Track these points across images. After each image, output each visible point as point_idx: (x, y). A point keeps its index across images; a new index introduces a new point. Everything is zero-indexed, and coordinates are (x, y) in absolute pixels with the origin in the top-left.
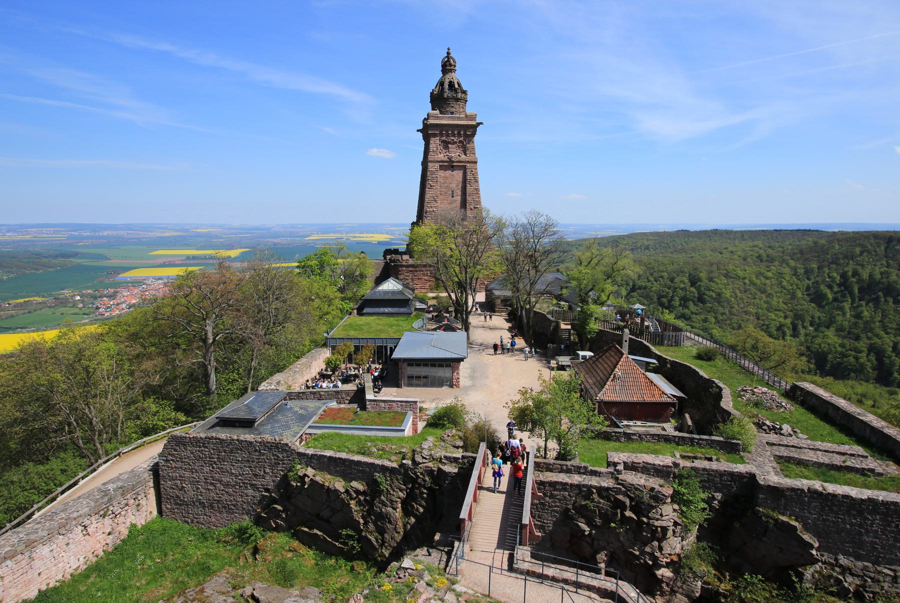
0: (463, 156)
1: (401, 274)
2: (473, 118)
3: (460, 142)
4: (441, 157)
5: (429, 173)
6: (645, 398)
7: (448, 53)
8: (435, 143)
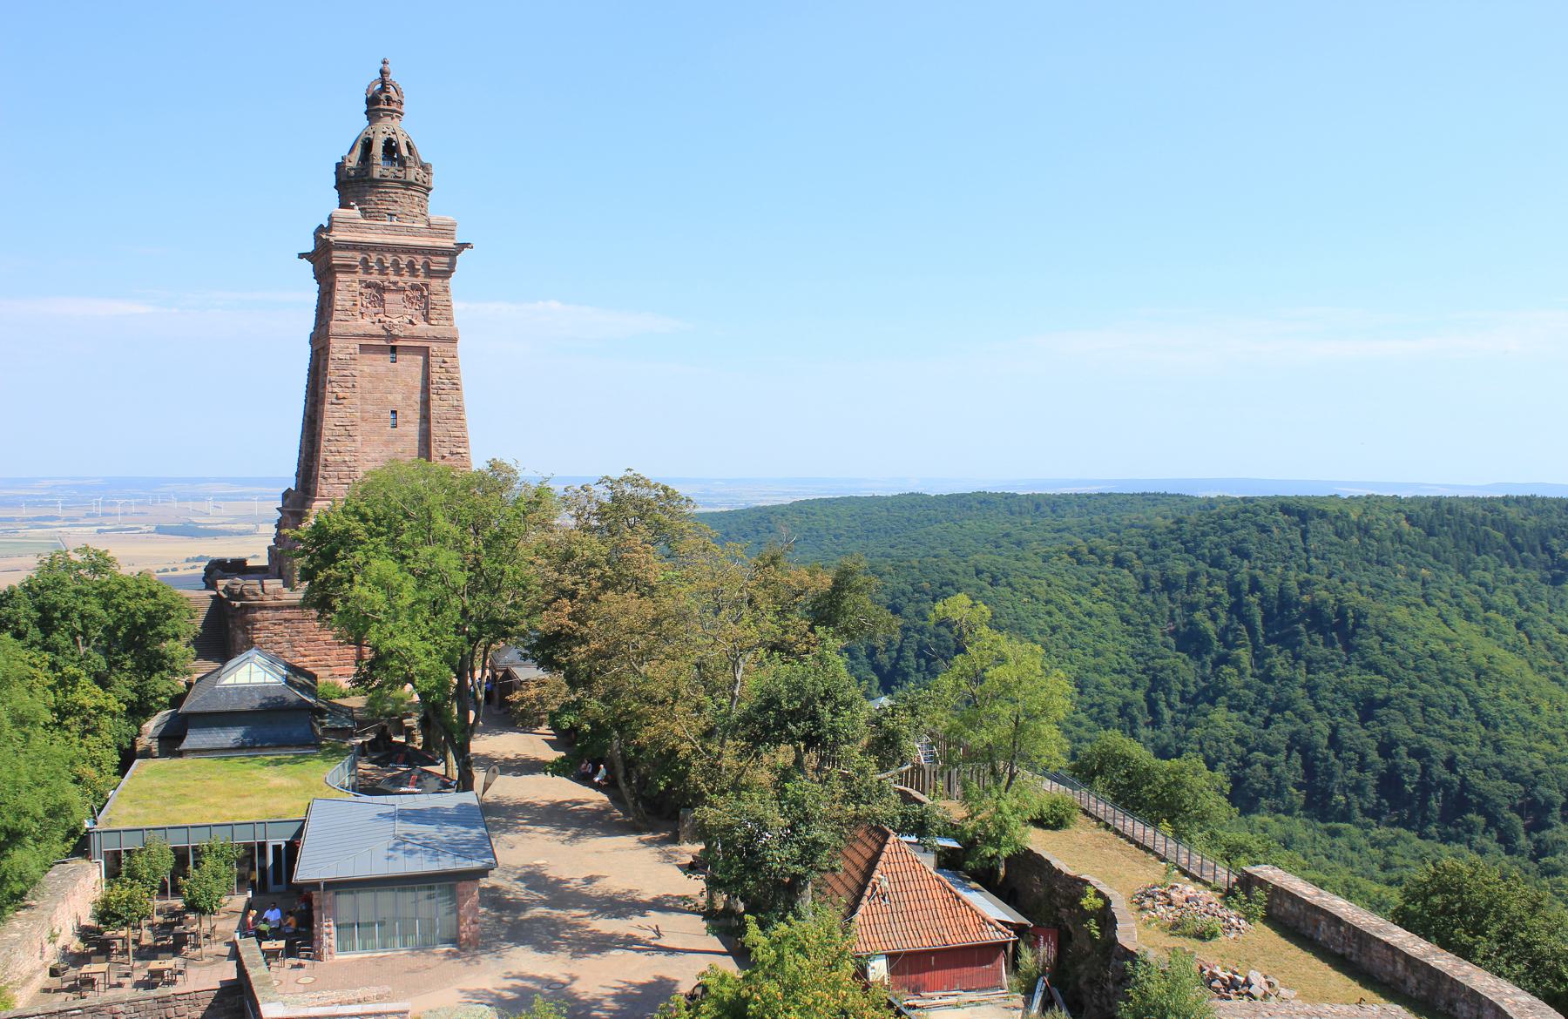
0: (421, 327)
2: (446, 230)
3: (414, 287)
4: (365, 324)
5: (331, 366)
6: (948, 938)
7: (382, 72)
8: (347, 288)
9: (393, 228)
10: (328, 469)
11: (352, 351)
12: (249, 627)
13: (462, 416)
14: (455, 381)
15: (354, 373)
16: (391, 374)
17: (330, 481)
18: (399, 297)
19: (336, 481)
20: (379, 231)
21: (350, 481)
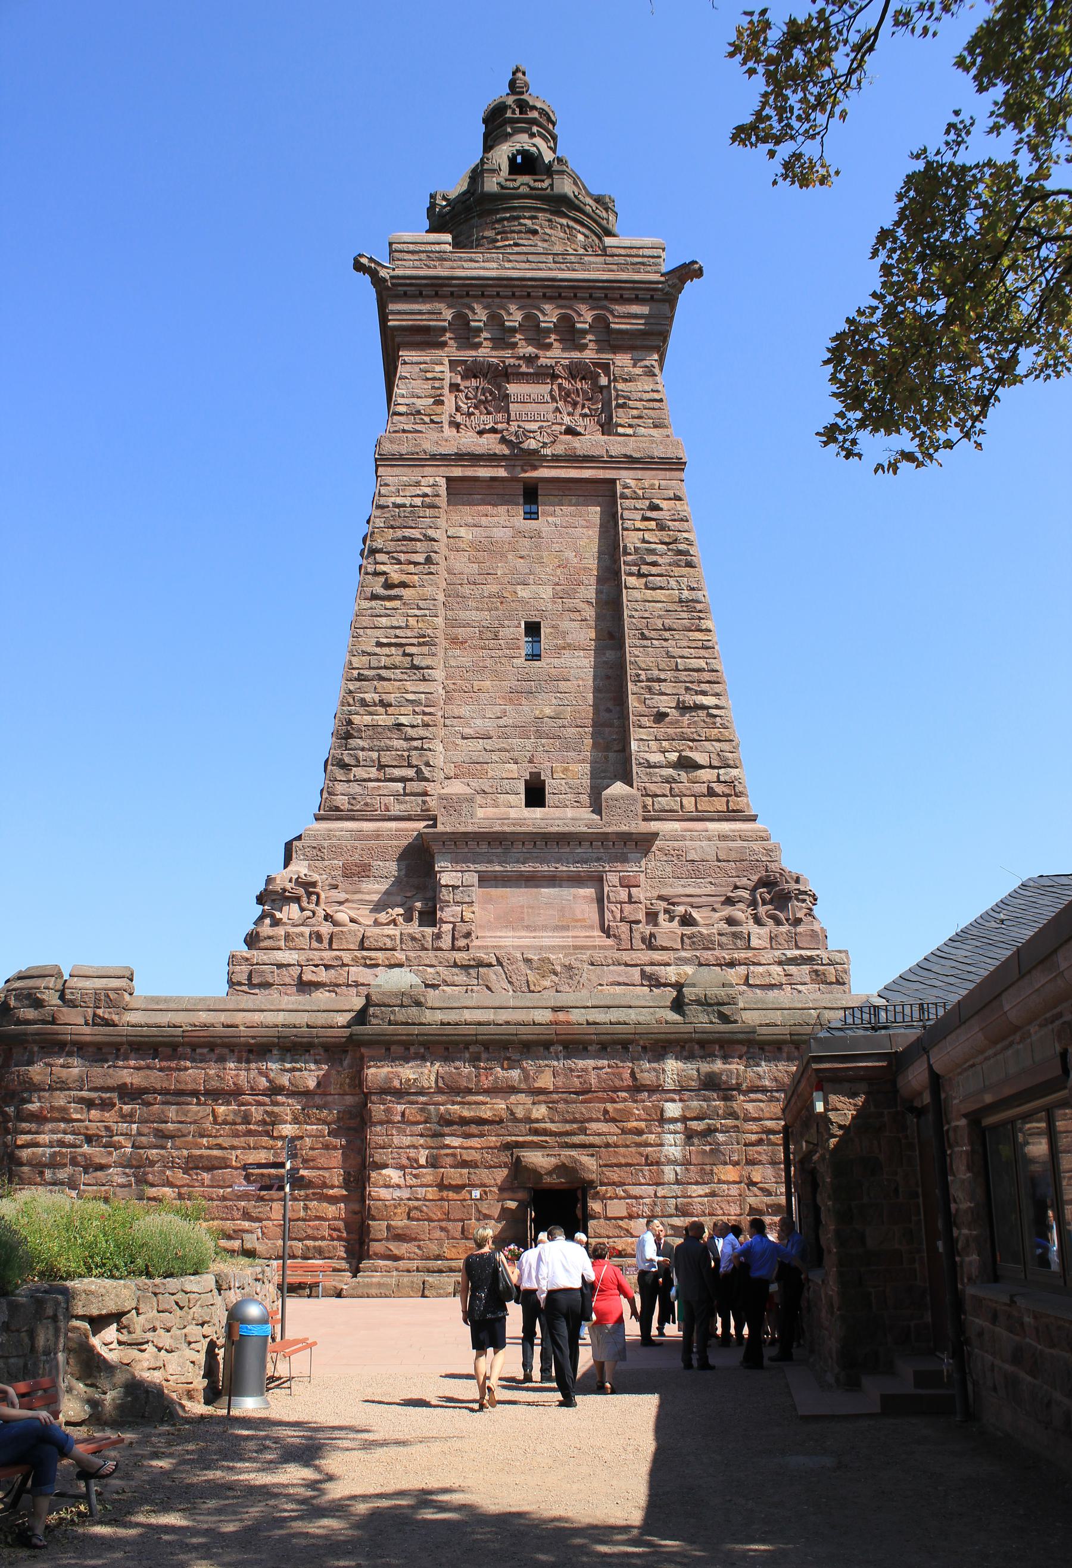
1: (39, 1118)
3: (576, 371)
9: (523, 258)
10: (353, 742)
11: (428, 490)
12: (10, 1110)
13: (705, 624)
14: (682, 547)
15: (431, 532)
16: (526, 542)
17: (359, 772)
18: (543, 389)
19: (373, 773)
20: (495, 265)
21: (411, 773)
